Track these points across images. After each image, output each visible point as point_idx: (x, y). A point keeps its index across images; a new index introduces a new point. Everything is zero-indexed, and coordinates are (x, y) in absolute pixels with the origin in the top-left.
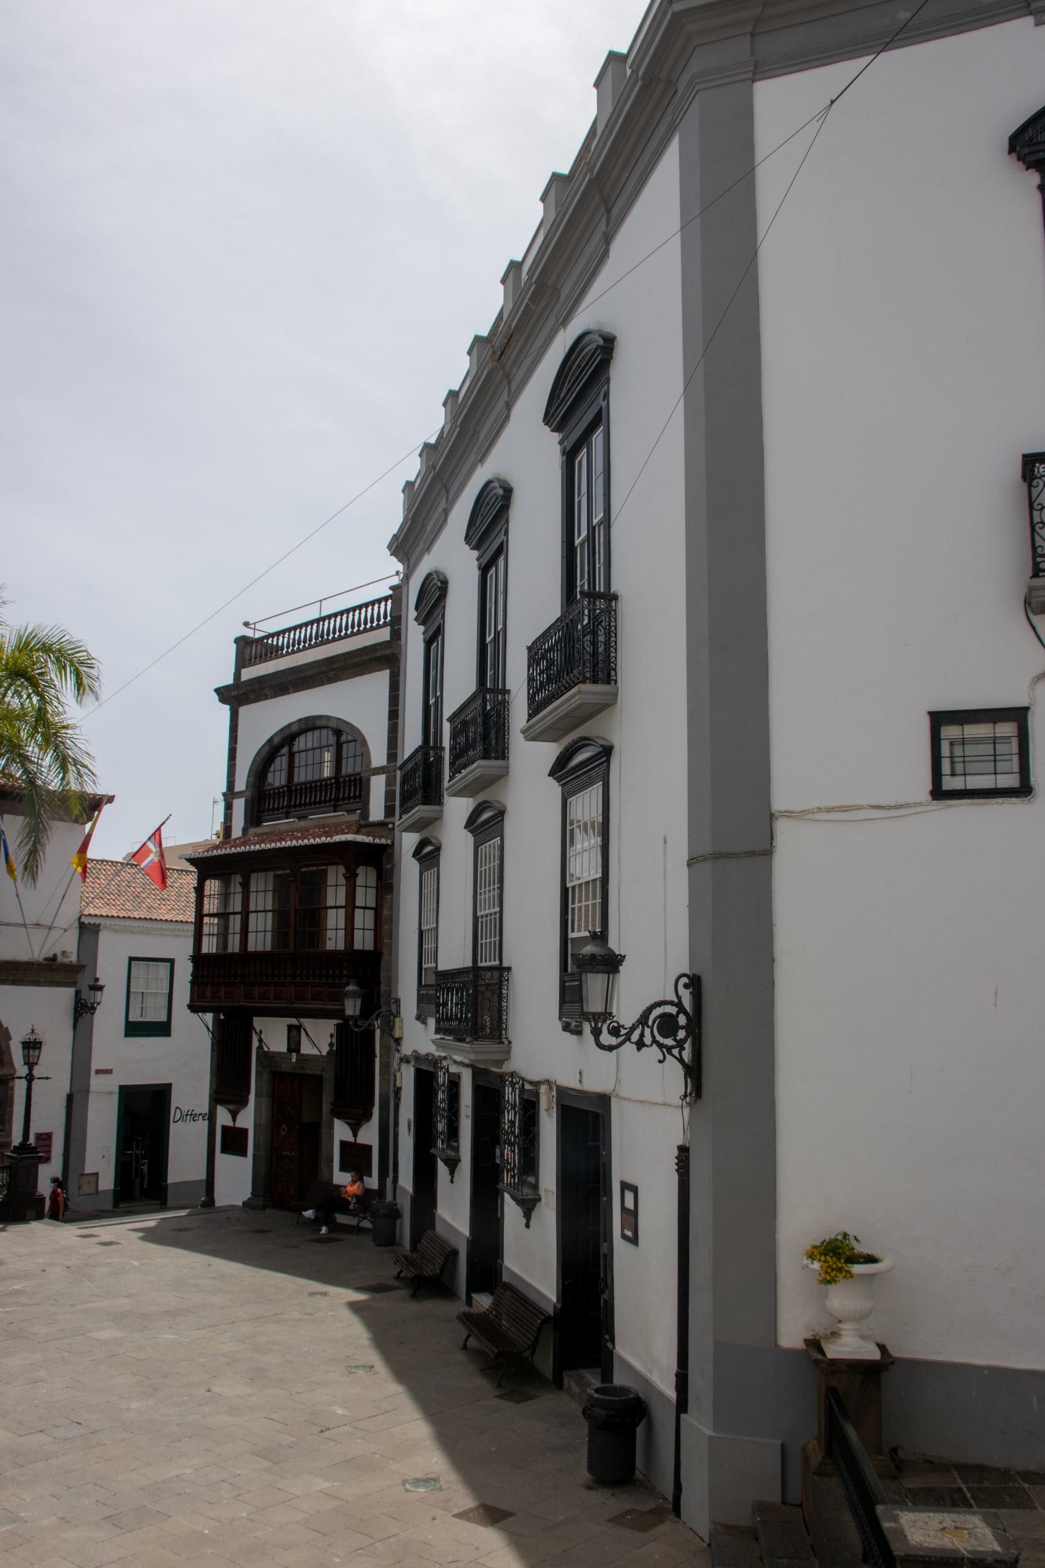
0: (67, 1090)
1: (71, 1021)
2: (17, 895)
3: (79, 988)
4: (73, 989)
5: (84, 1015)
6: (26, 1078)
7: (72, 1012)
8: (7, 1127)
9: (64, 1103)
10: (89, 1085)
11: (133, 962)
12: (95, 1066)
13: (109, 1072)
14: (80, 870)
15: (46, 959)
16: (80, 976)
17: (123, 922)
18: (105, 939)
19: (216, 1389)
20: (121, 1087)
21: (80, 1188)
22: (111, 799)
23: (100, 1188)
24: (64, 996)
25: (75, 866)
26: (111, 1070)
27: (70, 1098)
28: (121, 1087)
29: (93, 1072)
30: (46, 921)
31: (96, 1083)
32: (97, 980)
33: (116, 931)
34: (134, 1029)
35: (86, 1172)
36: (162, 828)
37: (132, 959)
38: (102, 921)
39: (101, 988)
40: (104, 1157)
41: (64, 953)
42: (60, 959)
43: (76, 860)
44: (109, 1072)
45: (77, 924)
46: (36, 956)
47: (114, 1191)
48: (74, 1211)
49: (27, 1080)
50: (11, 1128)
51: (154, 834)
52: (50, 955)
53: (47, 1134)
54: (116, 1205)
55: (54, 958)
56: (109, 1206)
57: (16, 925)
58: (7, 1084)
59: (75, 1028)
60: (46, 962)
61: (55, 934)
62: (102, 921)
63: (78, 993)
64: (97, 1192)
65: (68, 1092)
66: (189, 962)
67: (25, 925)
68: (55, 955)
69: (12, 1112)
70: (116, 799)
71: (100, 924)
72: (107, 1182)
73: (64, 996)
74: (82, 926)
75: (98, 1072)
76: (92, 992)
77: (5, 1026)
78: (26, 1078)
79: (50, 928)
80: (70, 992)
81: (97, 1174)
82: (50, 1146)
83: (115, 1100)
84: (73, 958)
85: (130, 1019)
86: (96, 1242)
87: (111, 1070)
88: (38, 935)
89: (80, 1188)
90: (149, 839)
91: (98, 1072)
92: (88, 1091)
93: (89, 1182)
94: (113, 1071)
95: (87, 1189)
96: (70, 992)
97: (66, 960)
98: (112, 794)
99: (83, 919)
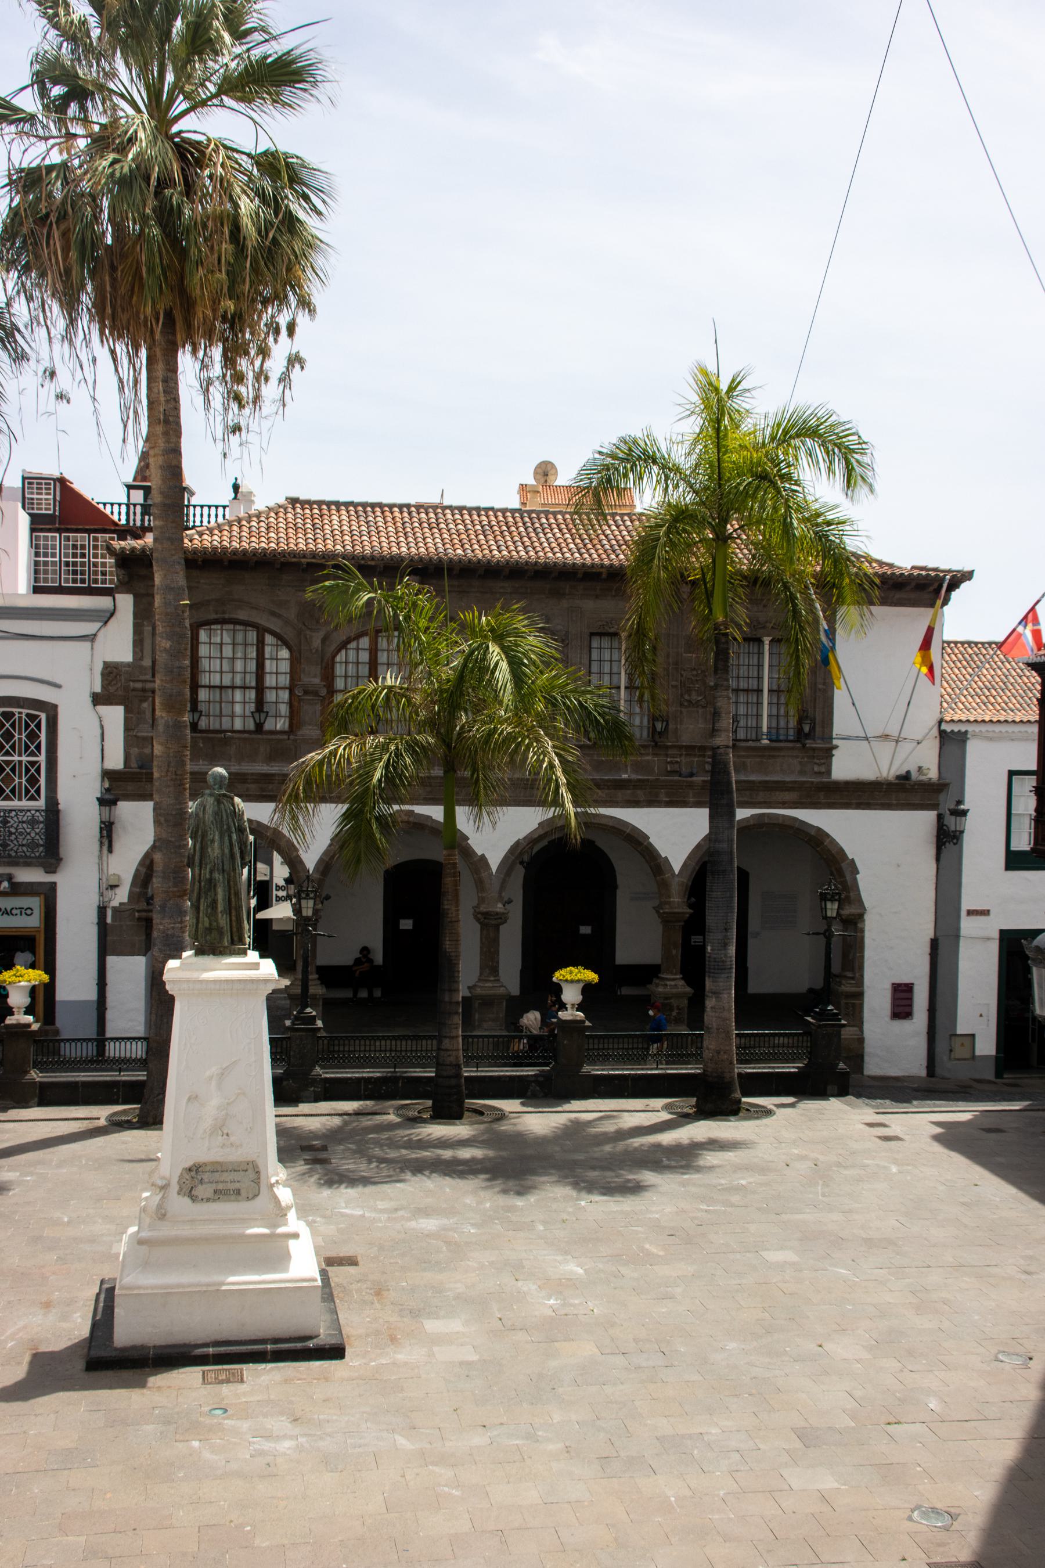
0: (930, 934)
1: (933, 851)
2: (854, 704)
3: (941, 811)
4: (935, 813)
5: (947, 844)
6: (824, 934)
7: (934, 840)
8: (857, 975)
9: (928, 950)
10: (958, 929)
11: (1014, 777)
12: (965, 906)
13: (985, 913)
14: (924, 670)
15: (898, 777)
16: (942, 797)
17: (998, 728)
18: (974, 749)
19: (829, 1346)
20: (1002, 932)
21: (951, 1051)
22: (968, 576)
23: (978, 1053)
24: (923, 821)
25: (918, 666)
26: (988, 911)
27: (934, 944)
28: (1002, 932)
29: (963, 913)
30: (893, 731)
31: (968, 926)
32: (960, 802)
33: (991, 739)
34: (1015, 861)
35: (959, 1032)
36: (1037, 607)
37: (1012, 774)
38: (970, 728)
39: (964, 813)
40: (981, 1016)
41: (920, 768)
42: (914, 776)
43: (919, 659)
44: (985, 913)
45: (935, 732)
46: (885, 774)
47: (997, 1057)
48: (943, 1078)
49: (826, 937)
50: (862, 976)
51: (1025, 617)
52: (902, 771)
53: (906, 985)
54: (999, 1074)
55: (907, 776)
56: (989, 1074)
57: (857, 738)
58: (855, 924)
59: (938, 859)
60: (897, 781)
61: (905, 748)
62: (970, 728)
63: (940, 817)
64: (974, 1057)
65: (932, 936)
66: (1032, 794)
67: (866, 738)
68: (908, 772)
69: (862, 957)
70: (975, 574)
71: (966, 732)
72: (986, 1045)
73: (923, 821)
74: (942, 734)
75: (970, 913)
76: (953, 818)
77: (850, 858)
78: (824, 934)
79: (897, 741)
80: (930, 816)
81: (973, 1036)
82: (911, 999)
83: (994, 948)
84: (933, 774)
85: (1013, 848)
86: (880, 1134)
87: (988, 911)
88: (885, 750)
89: (951, 1051)
90: (1020, 623)
91: (970, 913)
92: (957, 936)
93: (962, 1045)
94: (991, 912)
95: (960, 1052)
96: (930, 816)
97: (922, 778)
98: (970, 569)
99: (944, 727)
